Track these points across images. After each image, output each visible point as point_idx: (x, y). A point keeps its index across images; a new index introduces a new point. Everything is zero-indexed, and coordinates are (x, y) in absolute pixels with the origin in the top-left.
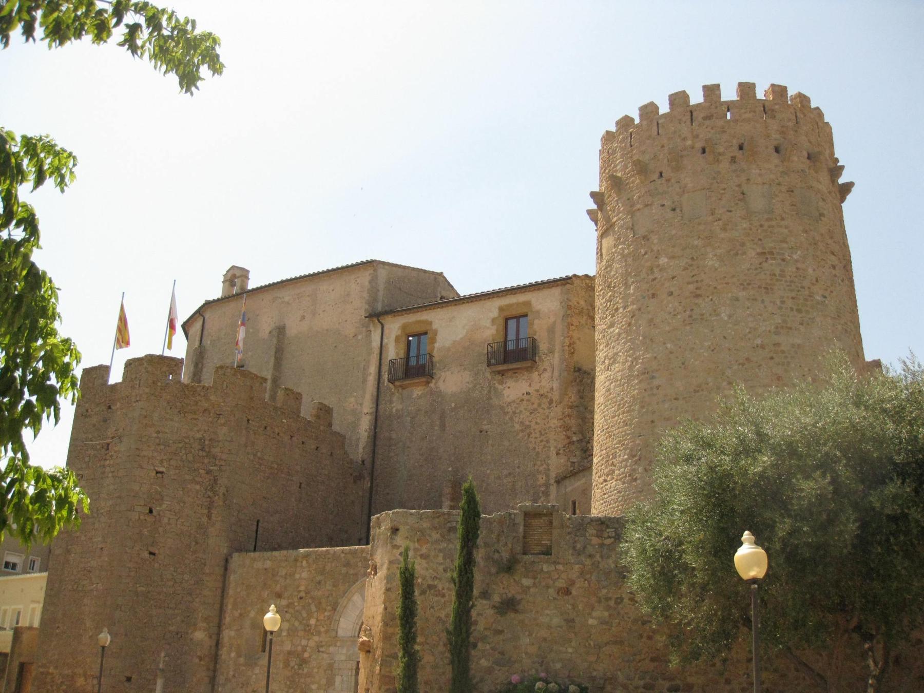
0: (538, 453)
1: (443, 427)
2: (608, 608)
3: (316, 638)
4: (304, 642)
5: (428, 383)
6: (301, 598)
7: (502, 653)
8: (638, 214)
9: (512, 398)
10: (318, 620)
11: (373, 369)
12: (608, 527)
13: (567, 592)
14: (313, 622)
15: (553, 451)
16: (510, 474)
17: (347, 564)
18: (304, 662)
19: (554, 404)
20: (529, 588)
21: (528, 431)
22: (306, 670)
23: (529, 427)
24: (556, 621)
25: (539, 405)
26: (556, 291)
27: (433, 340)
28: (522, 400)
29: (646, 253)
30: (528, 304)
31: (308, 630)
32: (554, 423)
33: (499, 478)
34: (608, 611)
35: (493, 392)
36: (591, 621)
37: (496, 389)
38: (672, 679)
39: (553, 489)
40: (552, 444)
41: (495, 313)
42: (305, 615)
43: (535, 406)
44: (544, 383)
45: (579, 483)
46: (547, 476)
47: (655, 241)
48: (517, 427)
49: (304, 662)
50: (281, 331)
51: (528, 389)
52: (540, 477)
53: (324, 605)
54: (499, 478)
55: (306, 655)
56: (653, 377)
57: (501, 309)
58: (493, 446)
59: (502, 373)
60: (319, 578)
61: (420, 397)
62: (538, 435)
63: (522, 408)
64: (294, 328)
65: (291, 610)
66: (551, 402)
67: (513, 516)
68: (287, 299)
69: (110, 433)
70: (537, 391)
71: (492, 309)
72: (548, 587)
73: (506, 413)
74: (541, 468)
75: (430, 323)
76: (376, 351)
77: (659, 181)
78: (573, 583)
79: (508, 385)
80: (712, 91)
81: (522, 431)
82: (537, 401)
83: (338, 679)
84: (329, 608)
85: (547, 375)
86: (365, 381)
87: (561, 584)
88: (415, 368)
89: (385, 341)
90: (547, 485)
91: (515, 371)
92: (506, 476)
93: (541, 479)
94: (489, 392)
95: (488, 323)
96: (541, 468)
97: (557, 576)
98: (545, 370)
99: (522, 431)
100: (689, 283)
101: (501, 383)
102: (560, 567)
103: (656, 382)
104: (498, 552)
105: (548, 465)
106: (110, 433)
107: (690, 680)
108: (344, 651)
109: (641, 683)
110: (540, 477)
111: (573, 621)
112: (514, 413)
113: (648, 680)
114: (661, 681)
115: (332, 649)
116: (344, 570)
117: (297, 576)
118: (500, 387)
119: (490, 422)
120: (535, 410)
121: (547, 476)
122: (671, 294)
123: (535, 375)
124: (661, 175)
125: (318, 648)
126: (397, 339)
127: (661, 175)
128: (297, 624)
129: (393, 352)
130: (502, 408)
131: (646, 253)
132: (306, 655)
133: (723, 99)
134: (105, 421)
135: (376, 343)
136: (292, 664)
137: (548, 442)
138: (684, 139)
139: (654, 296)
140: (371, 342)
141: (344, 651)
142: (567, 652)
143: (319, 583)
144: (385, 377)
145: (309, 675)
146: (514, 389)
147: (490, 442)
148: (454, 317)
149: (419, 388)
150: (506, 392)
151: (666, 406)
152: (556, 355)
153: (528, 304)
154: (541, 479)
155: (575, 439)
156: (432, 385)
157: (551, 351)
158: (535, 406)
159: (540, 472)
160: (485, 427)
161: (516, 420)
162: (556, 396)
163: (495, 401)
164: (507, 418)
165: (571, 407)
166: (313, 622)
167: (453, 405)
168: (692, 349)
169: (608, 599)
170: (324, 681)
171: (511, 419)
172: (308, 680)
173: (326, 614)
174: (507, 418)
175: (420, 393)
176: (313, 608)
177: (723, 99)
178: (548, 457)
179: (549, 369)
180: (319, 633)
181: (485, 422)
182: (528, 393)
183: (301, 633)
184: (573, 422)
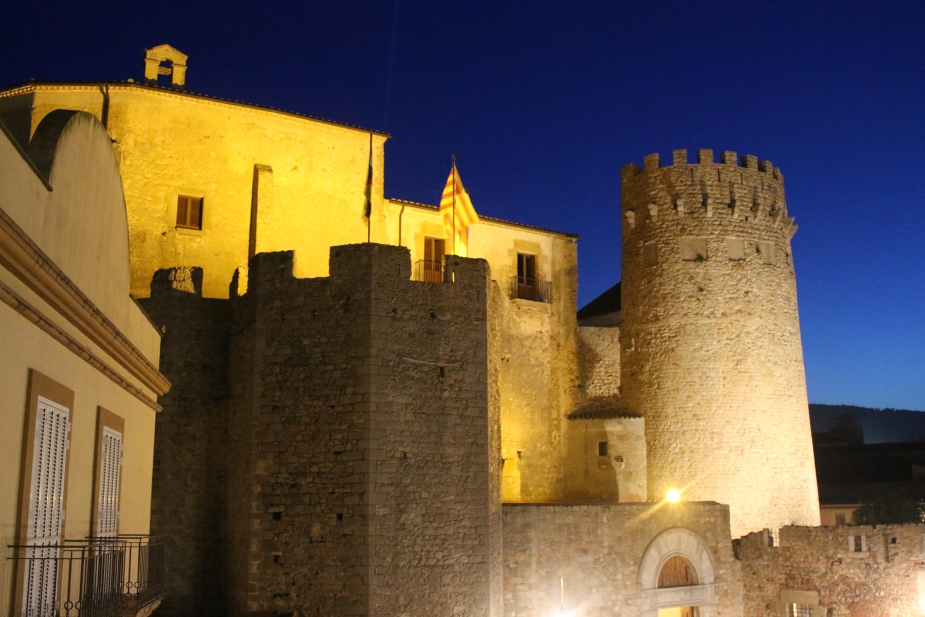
28: (536, 337)
35: (511, 324)
37: (514, 320)
40: (561, 383)
41: (511, 245)
48: (533, 361)
53: (627, 560)
57: (517, 243)
63: (536, 344)
84: (632, 562)
95: (506, 254)
108: (649, 601)
112: (530, 347)
115: (638, 601)
118: (517, 319)
119: (510, 352)
121: (559, 412)
137: (557, 380)
141: (649, 601)
143: (620, 538)
150: (523, 326)
160: (508, 356)
164: (524, 351)
178: (558, 395)
180: (626, 587)
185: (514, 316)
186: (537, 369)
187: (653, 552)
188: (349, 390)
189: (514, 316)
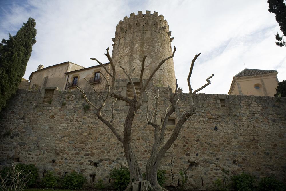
2: (68, 123)
7: (22, 140)
11: (65, 85)
12: (73, 94)
13: (53, 117)
20: (40, 115)
24: (47, 127)
27: (79, 78)
30: (100, 69)
34: (67, 124)
36: (60, 128)
38: (87, 151)
44: (102, 86)
50: (47, 78)
57: (94, 71)
64: (50, 76)
67: (40, 91)
68: (50, 71)
71: (92, 71)
72: (47, 115)
75: (79, 74)
76: (66, 81)
78: (55, 114)
80: (140, 12)
85: (102, 85)
86: (63, 88)
87: (52, 114)
88: (74, 84)
89: (69, 79)
97: (51, 111)
102: (53, 108)
104: (32, 103)
107: (94, 151)
109: (75, 152)
111: (53, 128)
113: (77, 151)
114: (82, 152)
123: (100, 85)
126: (71, 78)
129: (70, 81)
133: (143, 14)
135: (67, 80)
140: (65, 79)
142: (48, 140)
144: (67, 86)
169: (68, 120)
177: (143, 14)
179: (103, 83)
182: (98, 89)
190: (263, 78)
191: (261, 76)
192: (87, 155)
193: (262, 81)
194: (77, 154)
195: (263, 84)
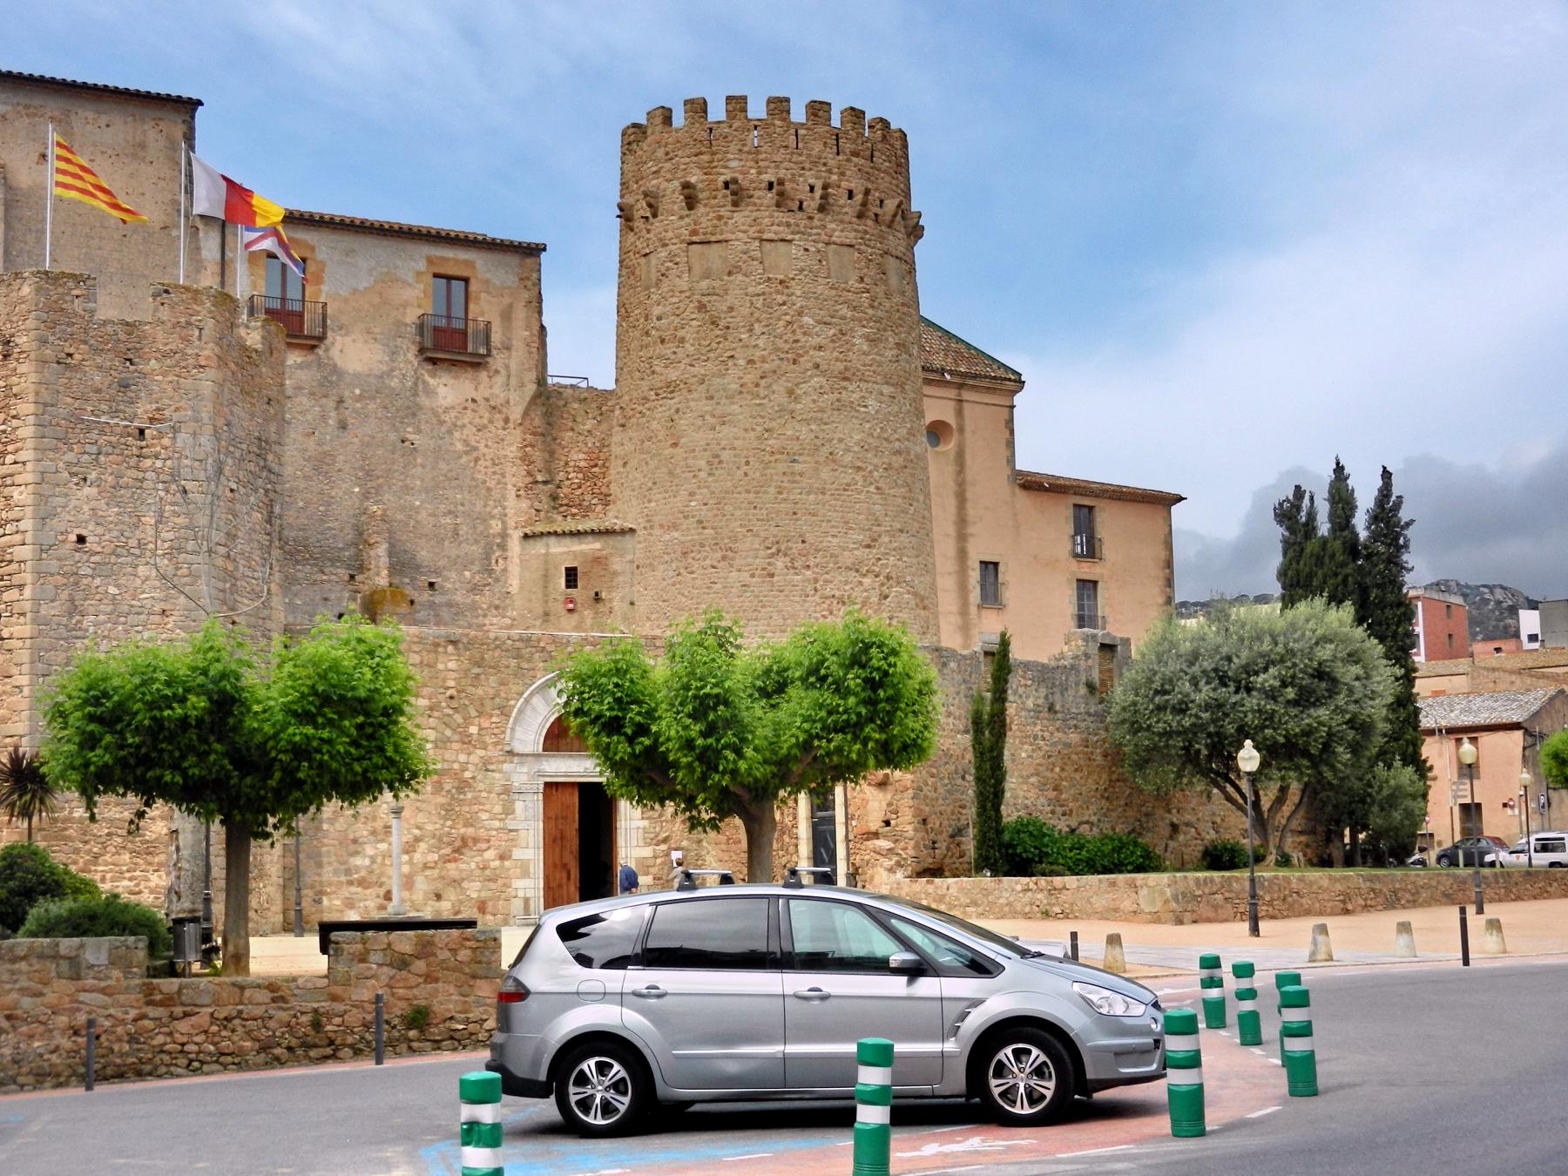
0: (489, 489)
1: (343, 426)
3: (481, 753)
4: (463, 758)
5: (313, 347)
6: (451, 697)
8: (767, 246)
9: (448, 402)
10: (481, 729)
14: (473, 730)
15: (512, 492)
16: (450, 512)
17: (518, 656)
18: (464, 785)
19: (511, 425)
21: (475, 454)
22: (469, 795)
23: (476, 449)
25: (491, 421)
26: (513, 260)
29: (784, 304)
30: (470, 264)
31: (466, 740)
32: (512, 450)
33: (433, 515)
35: (421, 387)
37: (424, 382)
39: (515, 544)
40: (510, 480)
41: (422, 265)
42: (460, 720)
43: (485, 421)
44: (497, 390)
45: (584, 547)
46: (504, 523)
47: (798, 293)
48: (459, 446)
49: (464, 785)
51: (474, 395)
52: (493, 523)
53: (488, 709)
54: (433, 515)
55: (467, 775)
56: (794, 461)
57: (430, 261)
58: (423, 466)
59: (434, 361)
60: (476, 670)
61: (300, 366)
62: (489, 463)
65: (436, 714)
66: (507, 420)
69: (144, 409)
70: (487, 400)
73: (442, 423)
74: (495, 511)
75: (313, 249)
77: (800, 215)
79: (444, 380)
81: (466, 453)
82: (487, 415)
83: (519, 806)
85: (500, 380)
89: (229, 254)
90: (504, 535)
91: (454, 363)
92: (445, 515)
93: (496, 526)
94: (416, 384)
96: (495, 511)
98: (497, 372)
99: (466, 453)
100: (837, 360)
101: (433, 376)
103: (798, 467)
105: (504, 508)
106: (144, 409)
108: (525, 769)
110: (493, 523)
115: (506, 767)
116: (513, 663)
117: (441, 666)
118: (431, 381)
119: (419, 431)
120: (485, 427)
121: (504, 523)
122: (817, 366)
123: (484, 375)
124: (800, 208)
125: (486, 766)
127: (800, 208)
128: (448, 733)
130: (436, 414)
131: (784, 304)
132: (467, 775)
134: (124, 386)
136: (447, 787)
137: (503, 475)
138: (830, 172)
139: (795, 362)
140: (198, 249)
145: (476, 800)
146: (448, 390)
147: (419, 461)
148: (353, 251)
149: (297, 352)
150: (442, 390)
151: (812, 497)
152: (514, 353)
153: (470, 264)
154: (496, 526)
155: (540, 478)
156: (320, 352)
157: (508, 348)
158: (485, 421)
159: (493, 517)
160: (410, 437)
161: (457, 435)
162: (516, 413)
163: (424, 400)
164: (444, 429)
165: (534, 434)
166: (473, 730)
167: (357, 392)
168: (841, 440)
170: (498, 809)
171: (450, 432)
172: (476, 808)
173: (494, 719)
174: (444, 429)
175: (299, 360)
176: (474, 713)
178: (504, 497)
179: (503, 372)
181: (410, 429)
182: (474, 401)
183: (456, 746)
184: (538, 455)
185: (427, 377)
186: (464, 459)
187: (536, 700)
188: (9, 459)
189: (427, 377)
190: (966, 395)
191: (960, 386)
192: (1064, 814)
193: (959, 413)
194: (1053, 812)
195: (961, 430)
